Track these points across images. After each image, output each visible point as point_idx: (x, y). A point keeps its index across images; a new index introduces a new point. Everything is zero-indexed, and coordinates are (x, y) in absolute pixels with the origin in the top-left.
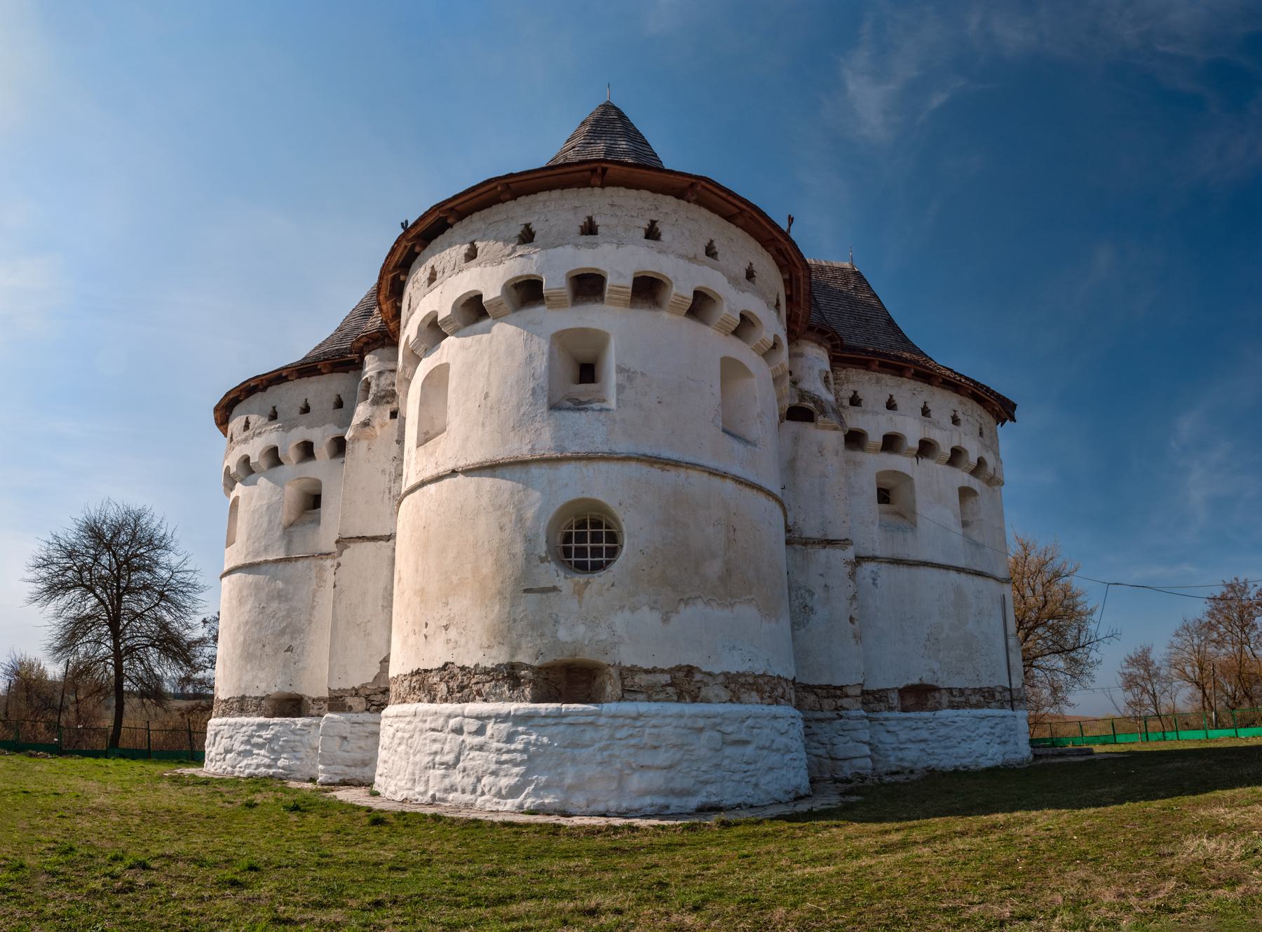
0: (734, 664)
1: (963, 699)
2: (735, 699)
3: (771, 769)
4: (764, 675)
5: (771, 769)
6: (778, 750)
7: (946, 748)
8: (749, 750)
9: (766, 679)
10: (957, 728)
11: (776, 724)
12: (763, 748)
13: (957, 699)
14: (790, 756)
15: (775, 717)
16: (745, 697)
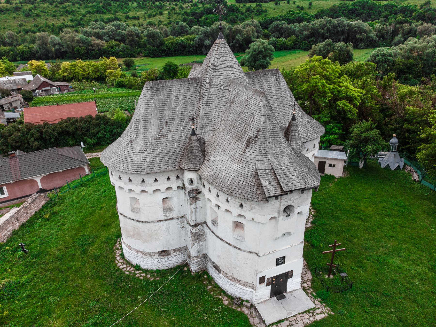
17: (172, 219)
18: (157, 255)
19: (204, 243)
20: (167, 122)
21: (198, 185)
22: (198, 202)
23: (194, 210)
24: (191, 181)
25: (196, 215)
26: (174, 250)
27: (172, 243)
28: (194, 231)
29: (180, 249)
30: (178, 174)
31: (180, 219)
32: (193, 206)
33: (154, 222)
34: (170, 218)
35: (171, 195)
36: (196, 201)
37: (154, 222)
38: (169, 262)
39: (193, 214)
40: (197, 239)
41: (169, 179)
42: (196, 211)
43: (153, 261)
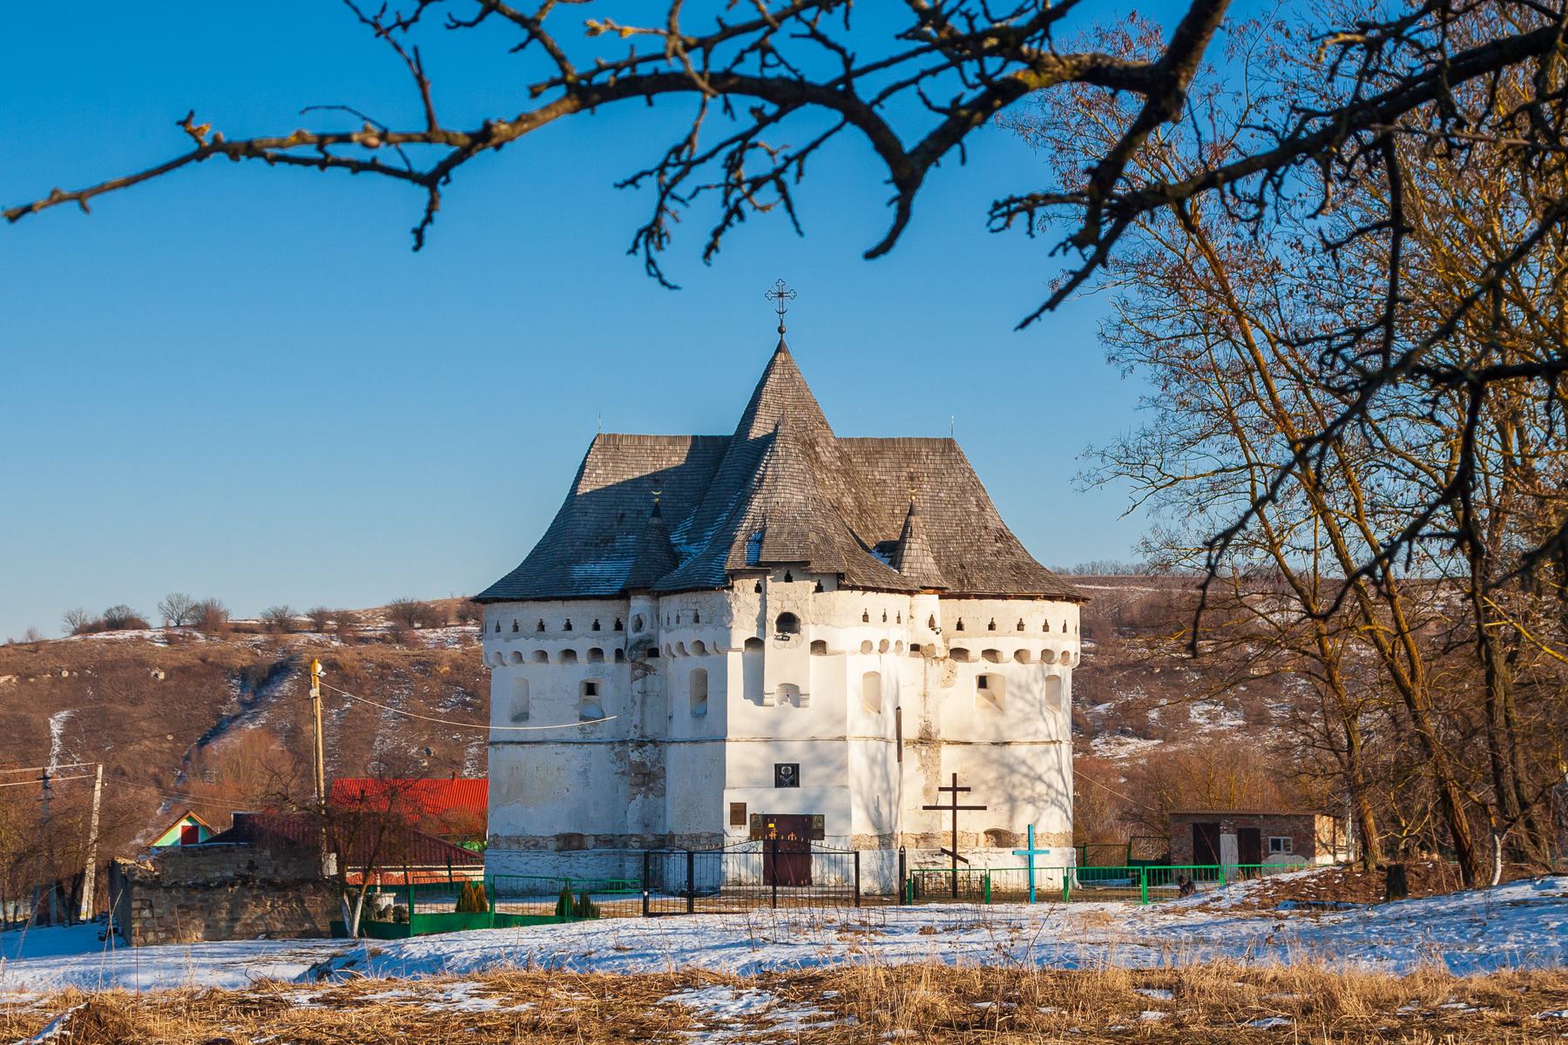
0: (507, 833)
19: (660, 801)
20: (623, 516)
21: (654, 631)
22: (649, 678)
23: (638, 698)
24: (639, 625)
25: (643, 712)
26: (596, 837)
27: (592, 813)
28: (635, 756)
31: (618, 748)
32: (638, 685)
33: (556, 742)
34: (593, 738)
37: (556, 742)
38: (581, 871)
39: (638, 707)
40: (643, 784)
41: (596, 627)
42: (643, 703)
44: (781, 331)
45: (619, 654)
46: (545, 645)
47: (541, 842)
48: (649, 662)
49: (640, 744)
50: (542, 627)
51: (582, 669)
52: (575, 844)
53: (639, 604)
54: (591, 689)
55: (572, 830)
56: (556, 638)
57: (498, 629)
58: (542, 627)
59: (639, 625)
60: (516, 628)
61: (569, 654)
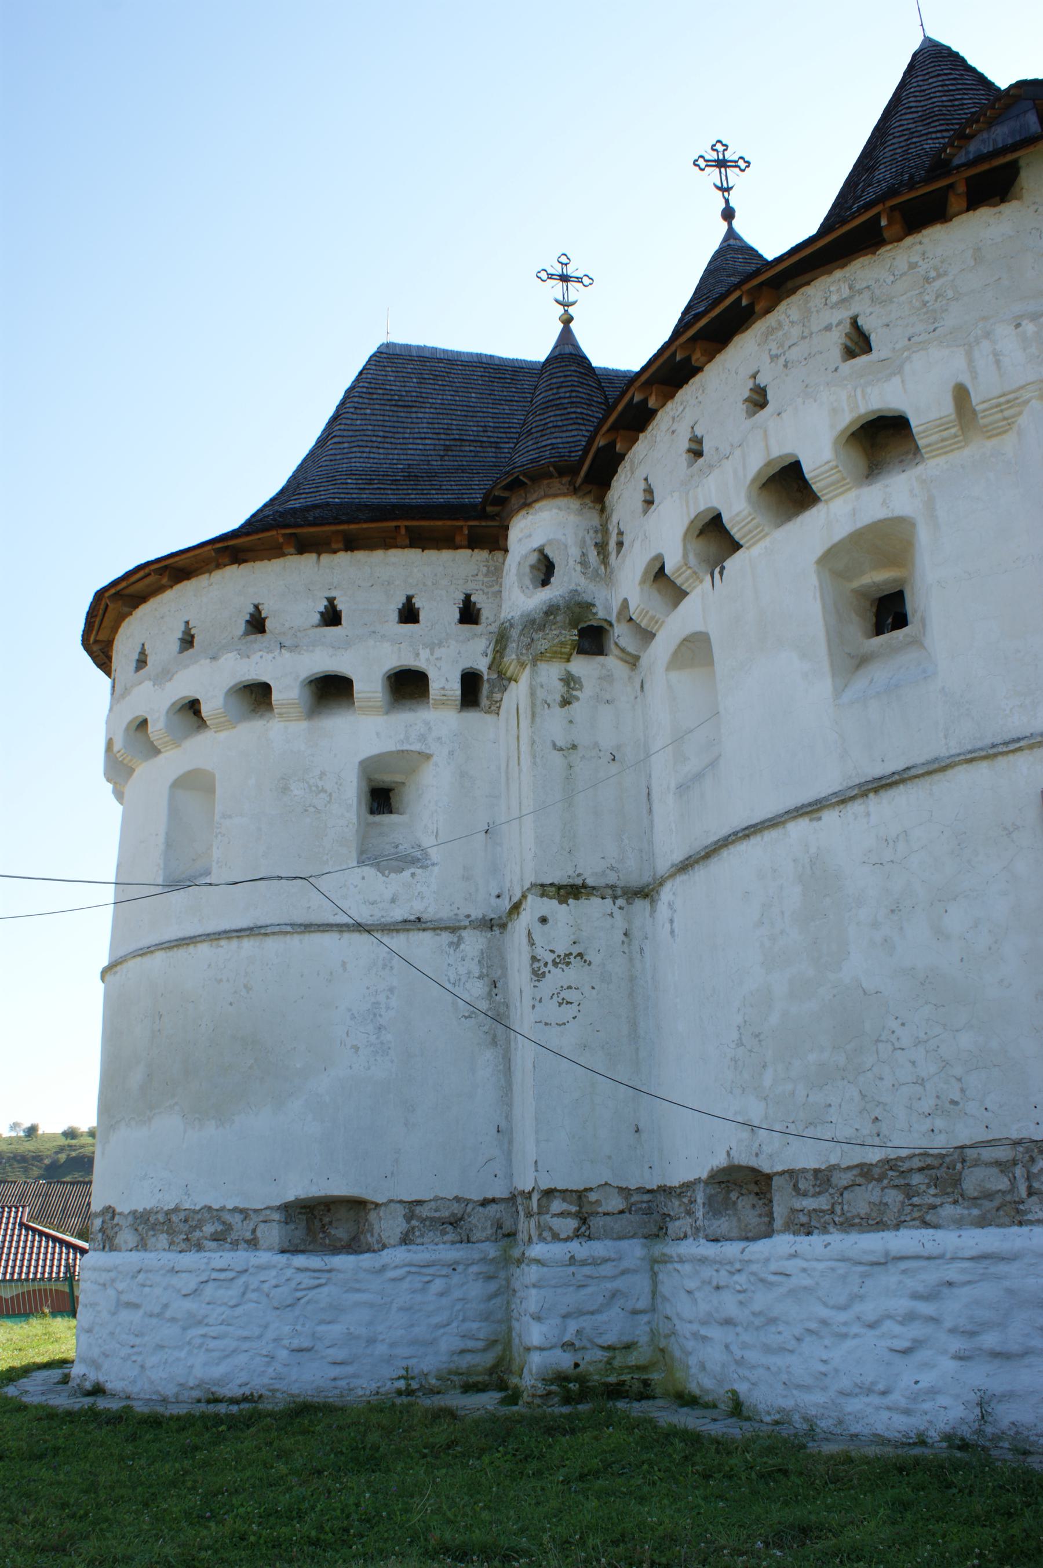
1: (822, 1202)
2: (142, 1245)
3: (160, 1347)
4: (176, 1210)
5: (160, 1347)
6: (173, 1320)
7: (767, 1349)
8: (135, 1317)
9: (182, 1215)
10: (792, 1292)
11: (175, 1280)
12: (151, 1316)
13: (809, 1203)
14: (203, 1330)
15: (174, 1271)
16: (151, 1241)
17: (417, 924)
18: (272, 1233)
24: (545, 569)
29: (455, 1222)
30: (469, 587)
34: (398, 914)
35: (422, 738)
36: (566, 702)
41: (409, 614)
43: (232, 1293)
44: (728, 214)
45: (471, 690)
46: (260, 664)
47: (242, 1229)
48: (581, 666)
49: (571, 891)
50: (257, 624)
51: (368, 731)
52: (340, 1232)
53: (543, 525)
54: (381, 798)
55: (339, 1187)
56: (295, 648)
57: (142, 662)
58: (257, 624)
59: (545, 569)
60: (188, 641)
61: (331, 690)
